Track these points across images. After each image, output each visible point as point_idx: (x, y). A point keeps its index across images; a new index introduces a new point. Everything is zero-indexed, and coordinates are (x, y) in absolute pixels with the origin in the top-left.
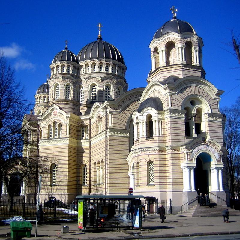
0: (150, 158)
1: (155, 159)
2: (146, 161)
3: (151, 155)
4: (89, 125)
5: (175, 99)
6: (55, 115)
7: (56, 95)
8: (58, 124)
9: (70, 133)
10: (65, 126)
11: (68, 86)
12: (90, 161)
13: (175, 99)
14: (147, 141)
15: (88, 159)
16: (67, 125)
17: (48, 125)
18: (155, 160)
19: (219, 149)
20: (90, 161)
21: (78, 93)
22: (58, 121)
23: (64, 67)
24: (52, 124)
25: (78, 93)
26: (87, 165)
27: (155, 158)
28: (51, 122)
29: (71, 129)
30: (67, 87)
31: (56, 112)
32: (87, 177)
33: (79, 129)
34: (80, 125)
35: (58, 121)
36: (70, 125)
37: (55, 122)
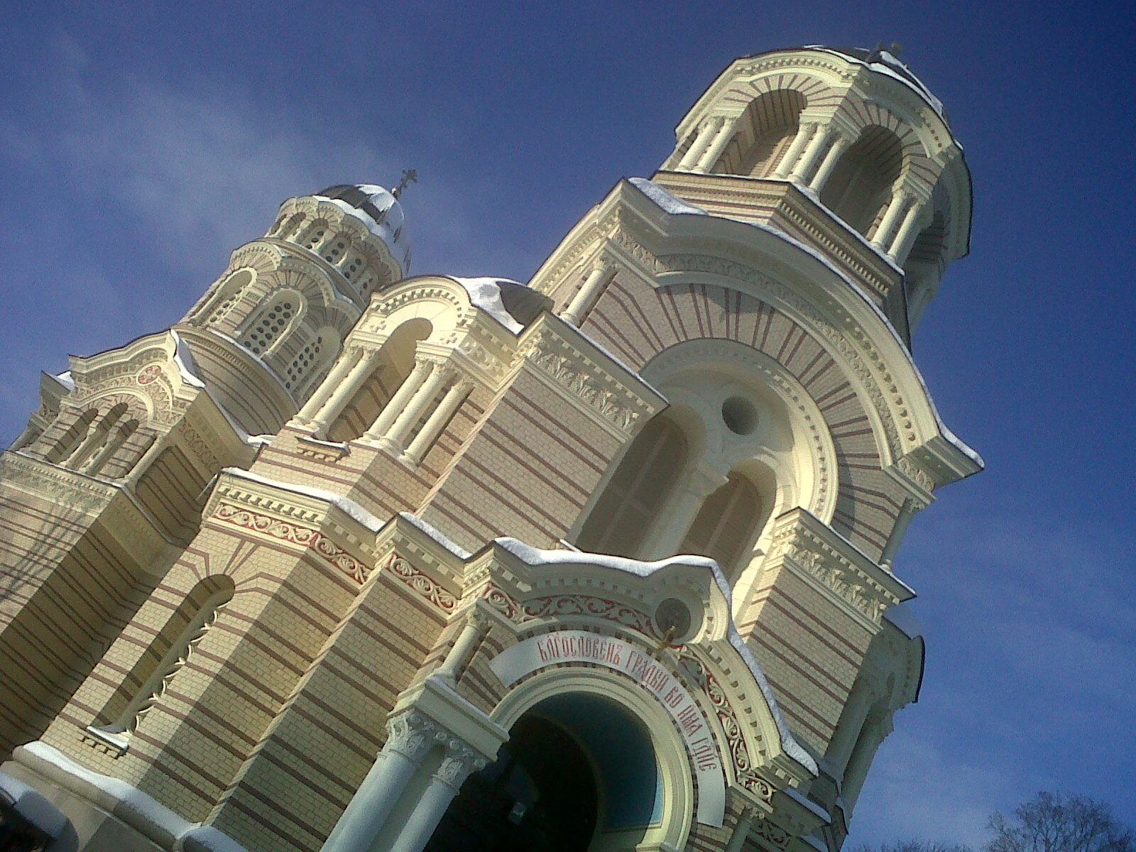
0: (238, 559)
1: (262, 583)
2: (201, 567)
3: (258, 543)
5: (628, 302)
9: (141, 480)
10: (143, 441)
11: (288, 306)
13: (628, 302)
14: (299, 456)
18: (252, 584)
19: (757, 762)
23: (321, 234)
27: (261, 575)
30: (278, 309)
35: (134, 408)
36: (168, 449)
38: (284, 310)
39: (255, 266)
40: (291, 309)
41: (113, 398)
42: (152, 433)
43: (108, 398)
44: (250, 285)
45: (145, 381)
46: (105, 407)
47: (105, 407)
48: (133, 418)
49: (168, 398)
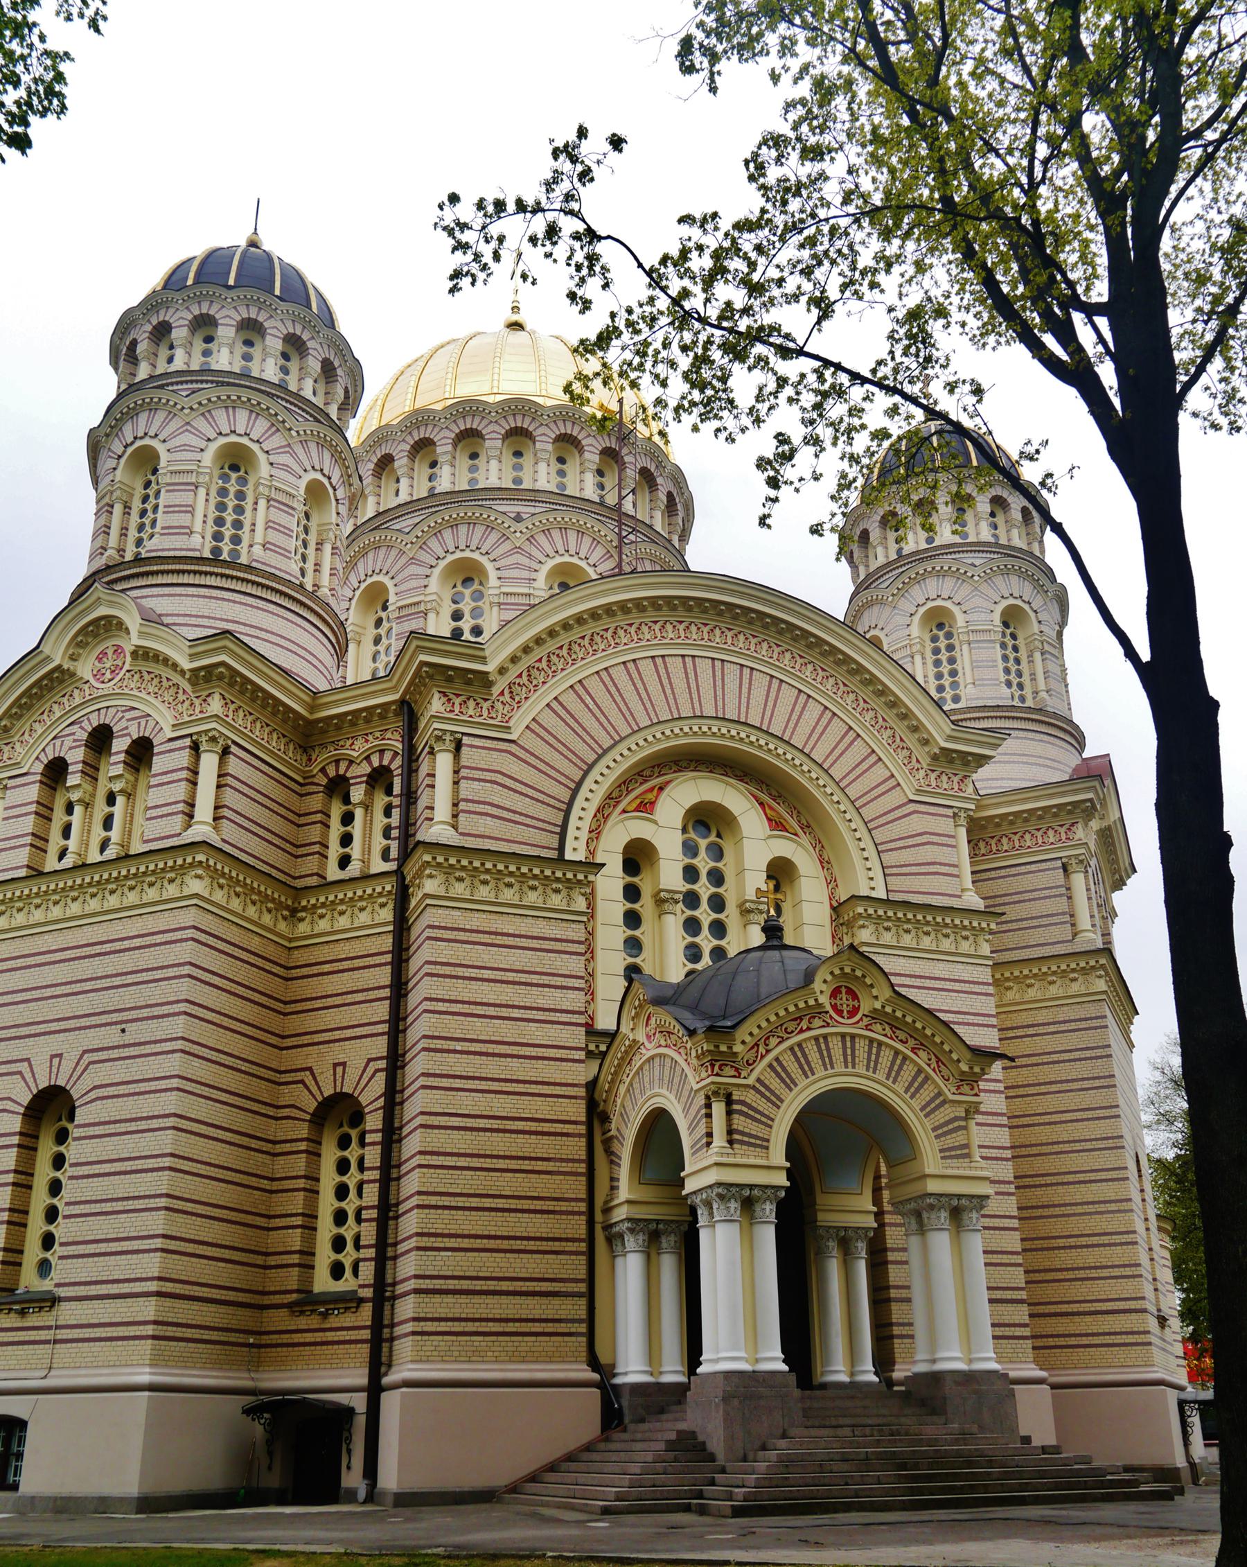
4: (398, 762)
6: (108, 675)
7: (133, 534)
8: (120, 744)
12: (395, 1060)
15: (380, 1046)
16: (195, 747)
17: (39, 767)
20: (395, 1060)
21: (320, 544)
22: (123, 724)
23: (209, 339)
24: (75, 756)
25: (320, 544)
26: (364, 1100)
28: (68, 742)
29: (229, 780)
31: (118, 650)
32: (365, 1214)
33: (316, 802)
34: (323, 770)
35: (123, 724)
37: (100, 739)
38: (234, 476)
39: (152, 433)
40: (243, 470)
41: (75, 728)
42: (187, 742)
43: (63, 733)
44: (163, 463)
45: (108, 675)
46: (71, 748)
47: (71, 748)
48: (135, 736)
49: (168, 679)
